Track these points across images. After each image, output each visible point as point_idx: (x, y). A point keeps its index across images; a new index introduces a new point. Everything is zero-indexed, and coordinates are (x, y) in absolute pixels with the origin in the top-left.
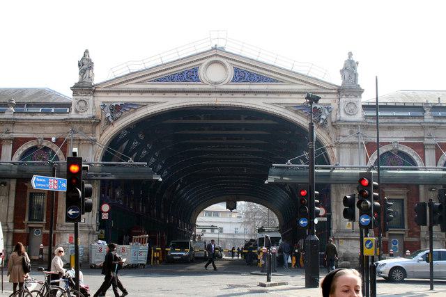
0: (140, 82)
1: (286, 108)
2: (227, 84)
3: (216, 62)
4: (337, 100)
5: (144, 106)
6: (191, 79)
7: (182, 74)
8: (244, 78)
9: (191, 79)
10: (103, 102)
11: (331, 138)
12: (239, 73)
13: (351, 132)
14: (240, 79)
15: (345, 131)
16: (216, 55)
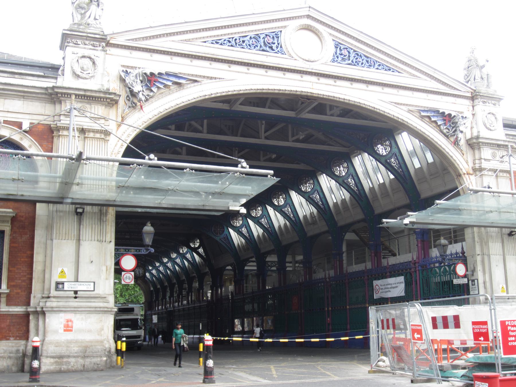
0: (189, 40)
1: (410, 111)
2: (325, 64)
3: (308, 28)
4: (471, 108)
5: (196, 81)
6: (271, 48)
7: (257, 37)
8: (349, 60)
9: (271, 48)
10: (123, 66)
11: (467, 162)
12: (341, 50)
13: (494, 156)
14: (343, 59)
15: (486, 153)
16: (309, 17)
